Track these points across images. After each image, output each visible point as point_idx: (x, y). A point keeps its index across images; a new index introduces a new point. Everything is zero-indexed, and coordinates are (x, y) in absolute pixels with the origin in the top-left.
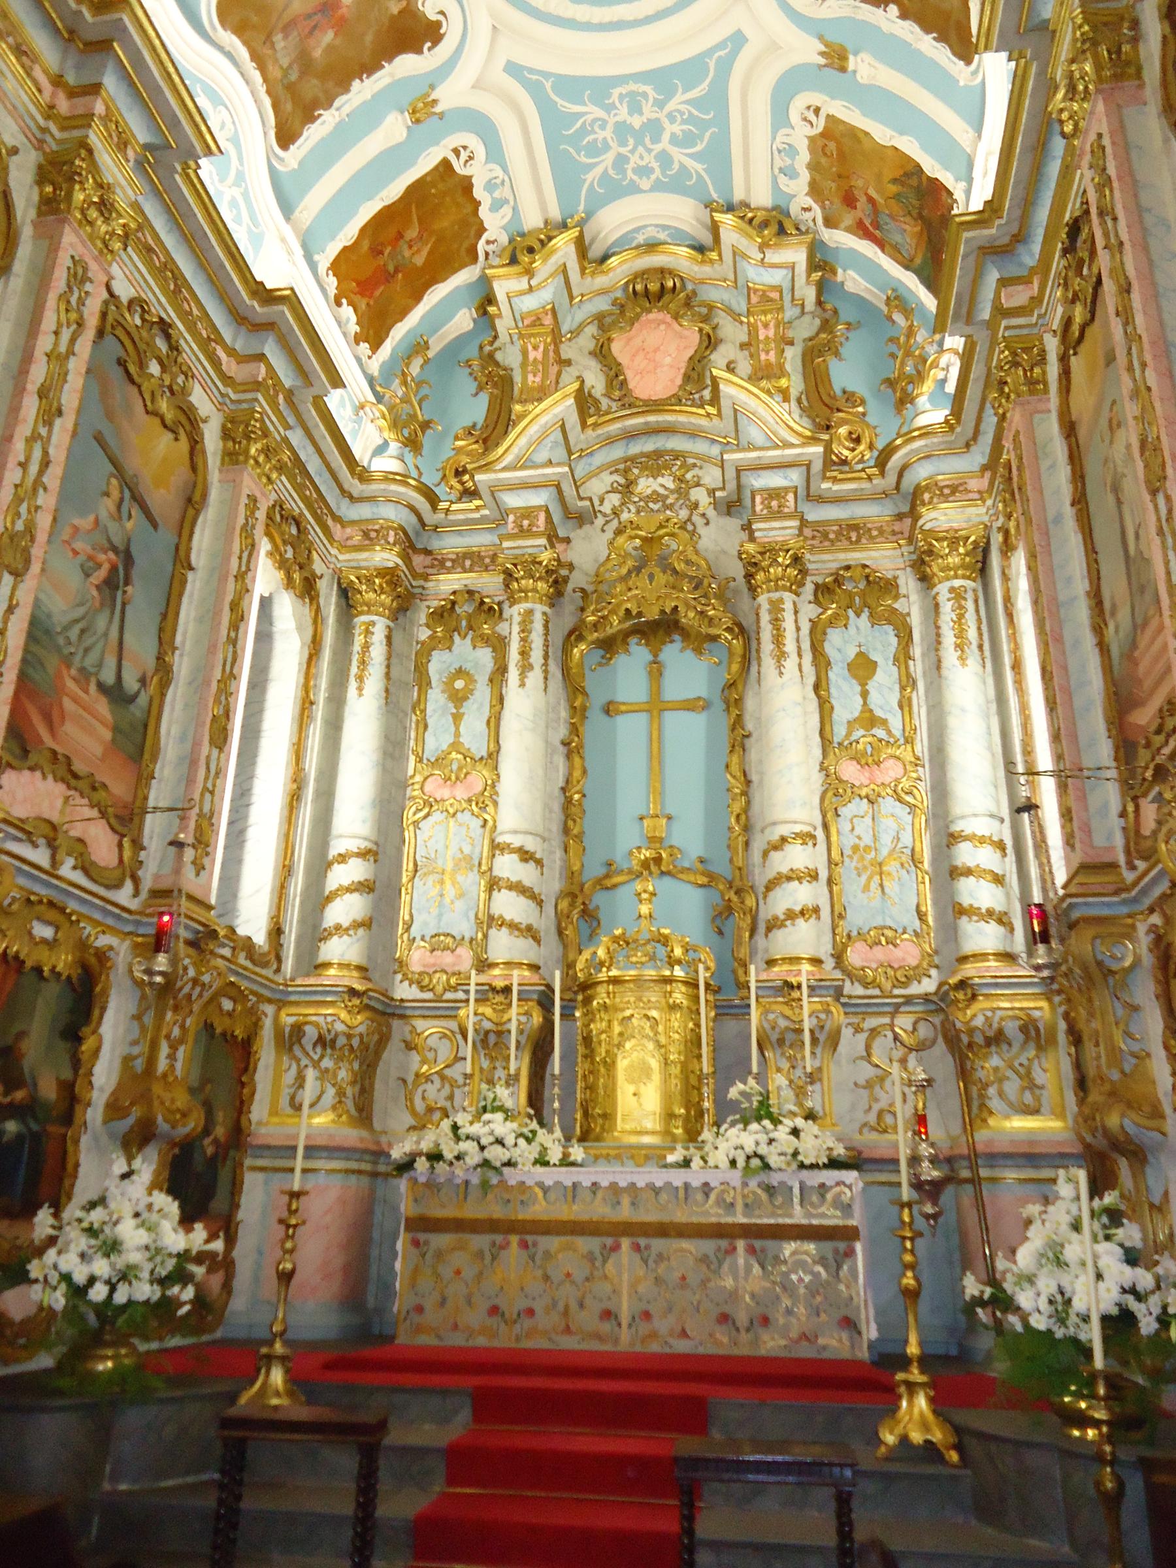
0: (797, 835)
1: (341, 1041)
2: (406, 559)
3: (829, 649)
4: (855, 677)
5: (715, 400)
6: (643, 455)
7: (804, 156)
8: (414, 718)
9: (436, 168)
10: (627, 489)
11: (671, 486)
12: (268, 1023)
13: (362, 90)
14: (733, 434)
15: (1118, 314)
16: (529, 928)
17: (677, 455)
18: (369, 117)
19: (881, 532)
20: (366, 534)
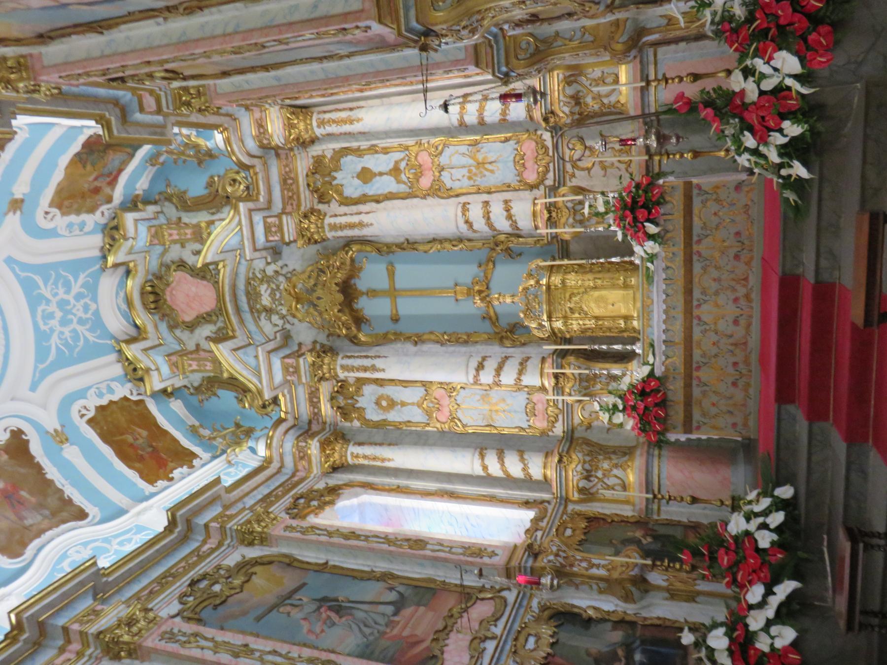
0: (464, 214)
1: (587, 466)
2: (313, 436)
4: (371, 180)
5: (216, 263)
6: (249, 303)
7: (73, 218)
8: (405, 428)
9: (93, 427)
10: (269, 311)
12: (578, 508)
13: (52, 473)
16: (521, 364)
18: (66, 467)
19: (287, 166)
20: (302, 458)
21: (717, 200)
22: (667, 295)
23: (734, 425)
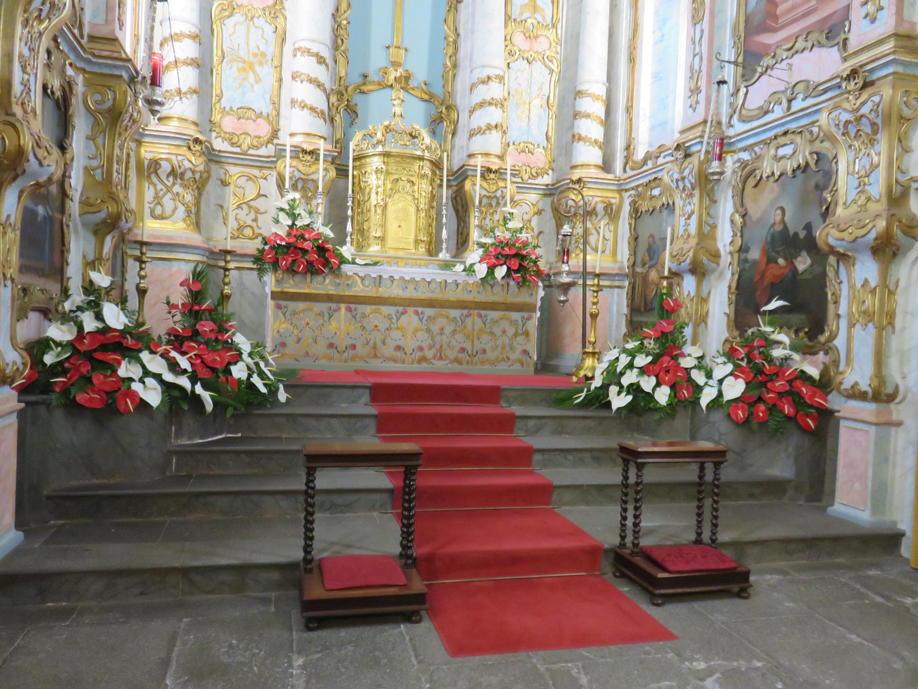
0: (497, 77)
1: (189, 175)
21: (516, 335)
22: (429, 283)
23: (283, 345)
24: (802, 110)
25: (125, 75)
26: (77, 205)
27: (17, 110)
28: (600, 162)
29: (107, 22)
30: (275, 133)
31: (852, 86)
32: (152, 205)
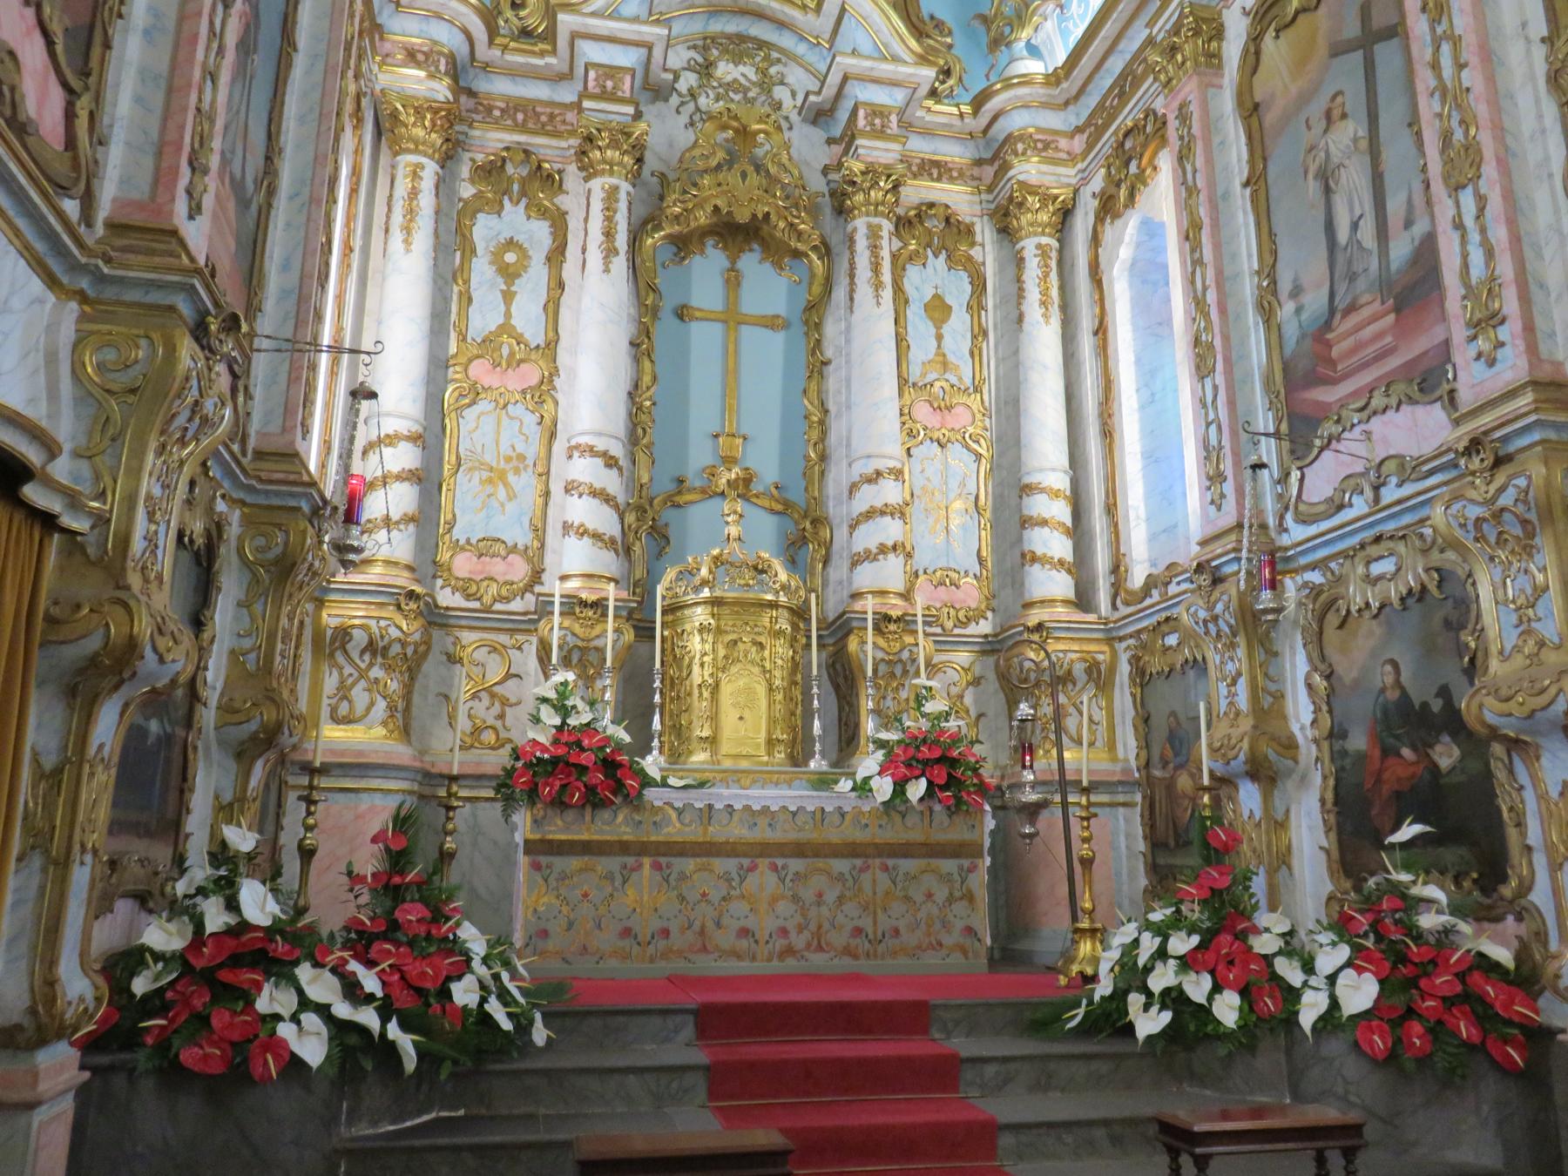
0: (891, 471)
1: (396, 649)
3: (908, 286)
4: (932, 319)
8: (456, 289)
10: (705, 70)
11: (753, 77)
14: (827, 36)
15: (1424, 9)
17: (762, 44)
21: (951, 900)
22: (794, 814)
23: (544, 934)
24: (1399, 502)
25: (305, 507)
26: (213, 712)
27: (134, 580)
28: (1070, 594)
29: (284, 430)
30: (537, 576)
31: (1475, 463)
32: (333, 701)
